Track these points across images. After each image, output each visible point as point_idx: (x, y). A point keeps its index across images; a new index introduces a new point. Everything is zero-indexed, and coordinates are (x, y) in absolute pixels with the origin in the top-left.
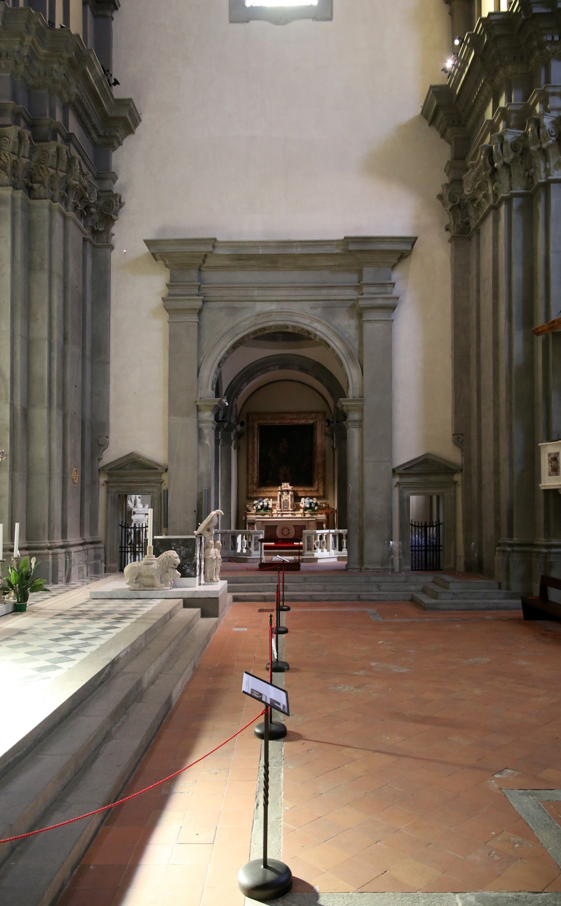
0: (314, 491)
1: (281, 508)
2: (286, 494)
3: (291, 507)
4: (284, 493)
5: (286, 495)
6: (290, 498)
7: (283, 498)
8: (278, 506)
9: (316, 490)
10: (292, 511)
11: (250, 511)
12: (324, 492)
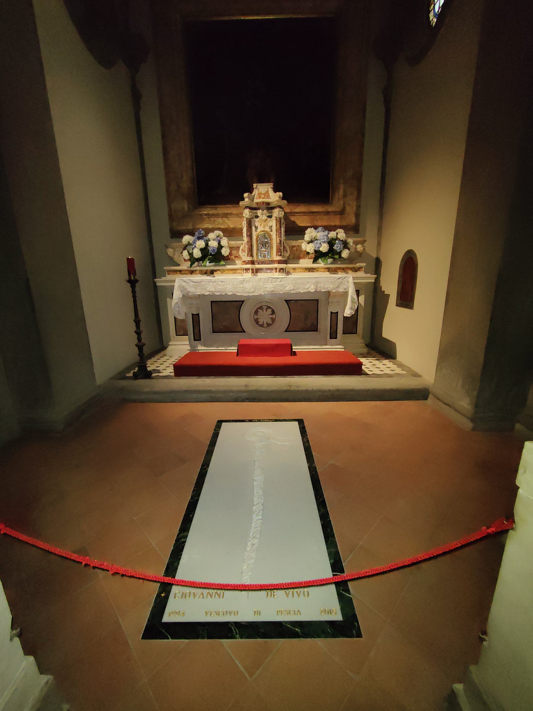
0: (335, 213)
1: (252, 256)
2: (265, 217)
3: (279, 251)
4: (259, 212)
5: (266, 220)
6: (274, 228)
7: (256, 228)
8: (243, 251)
9: (338, 210)
10: (279, 262)
11: (179, 265)
12: (357, 216)
